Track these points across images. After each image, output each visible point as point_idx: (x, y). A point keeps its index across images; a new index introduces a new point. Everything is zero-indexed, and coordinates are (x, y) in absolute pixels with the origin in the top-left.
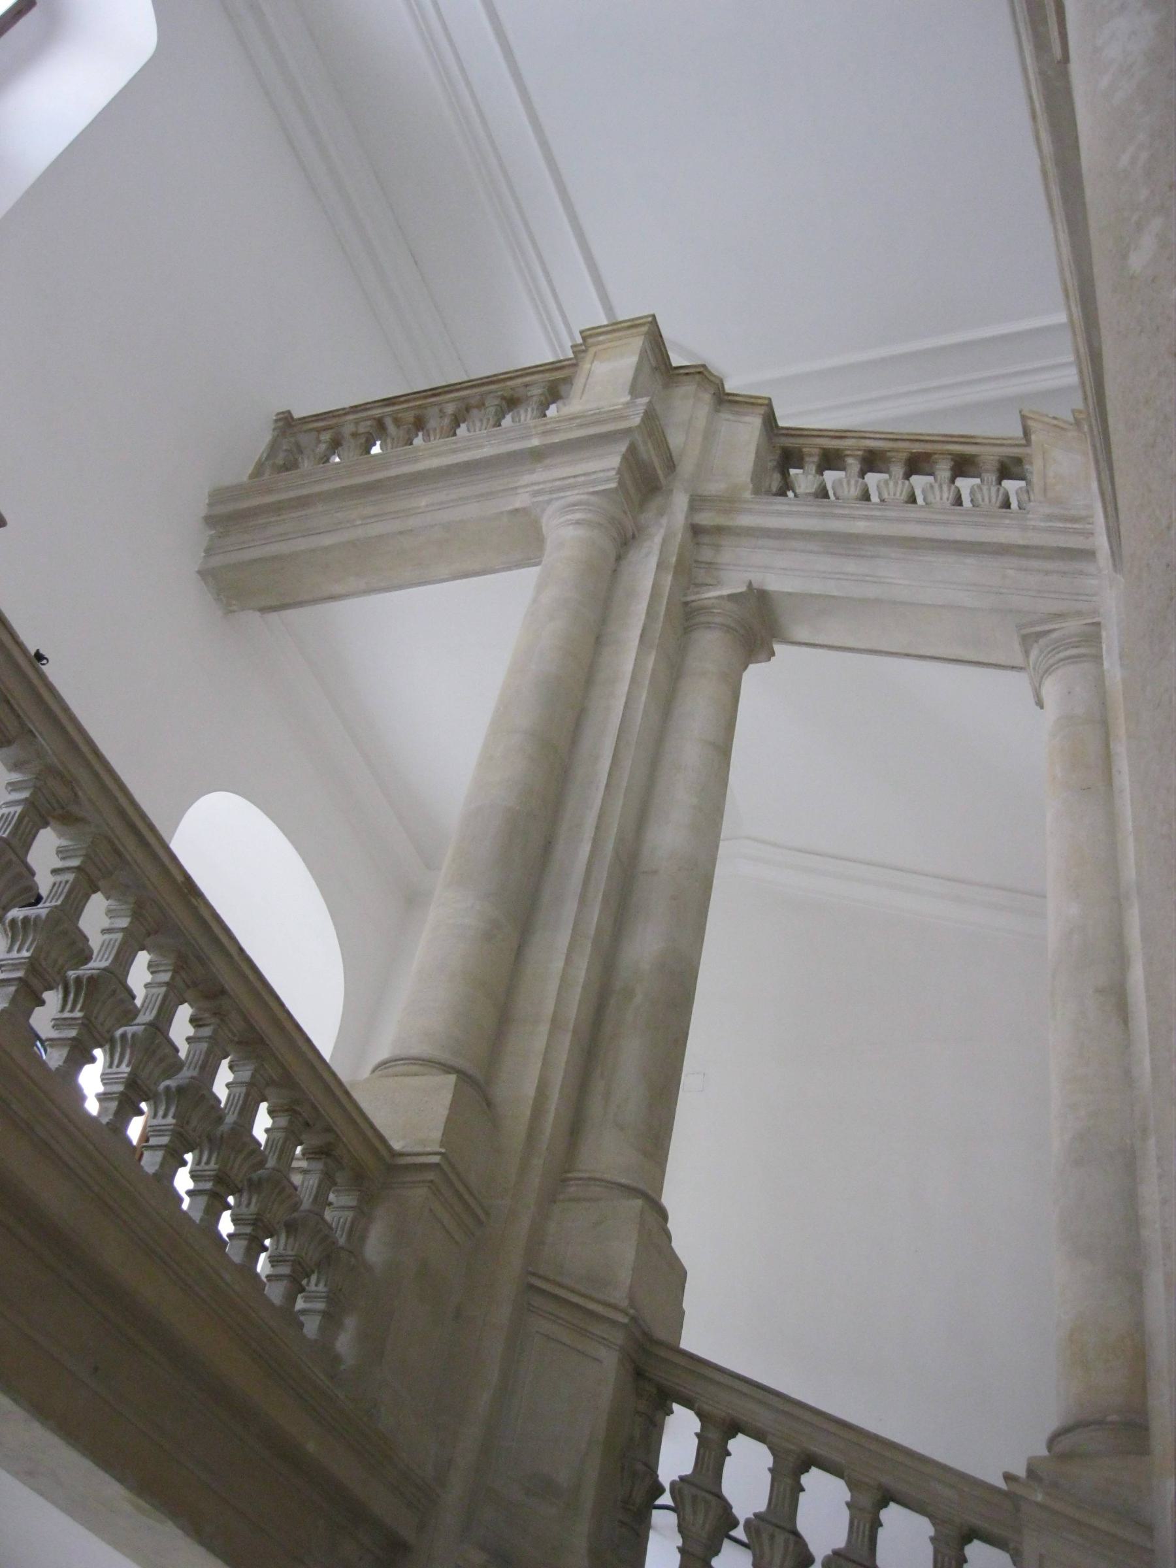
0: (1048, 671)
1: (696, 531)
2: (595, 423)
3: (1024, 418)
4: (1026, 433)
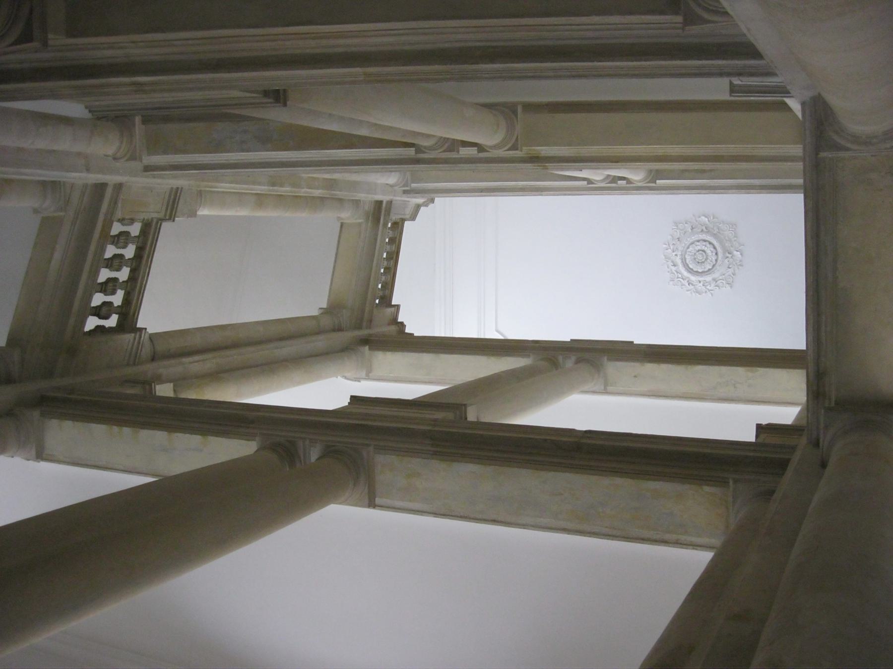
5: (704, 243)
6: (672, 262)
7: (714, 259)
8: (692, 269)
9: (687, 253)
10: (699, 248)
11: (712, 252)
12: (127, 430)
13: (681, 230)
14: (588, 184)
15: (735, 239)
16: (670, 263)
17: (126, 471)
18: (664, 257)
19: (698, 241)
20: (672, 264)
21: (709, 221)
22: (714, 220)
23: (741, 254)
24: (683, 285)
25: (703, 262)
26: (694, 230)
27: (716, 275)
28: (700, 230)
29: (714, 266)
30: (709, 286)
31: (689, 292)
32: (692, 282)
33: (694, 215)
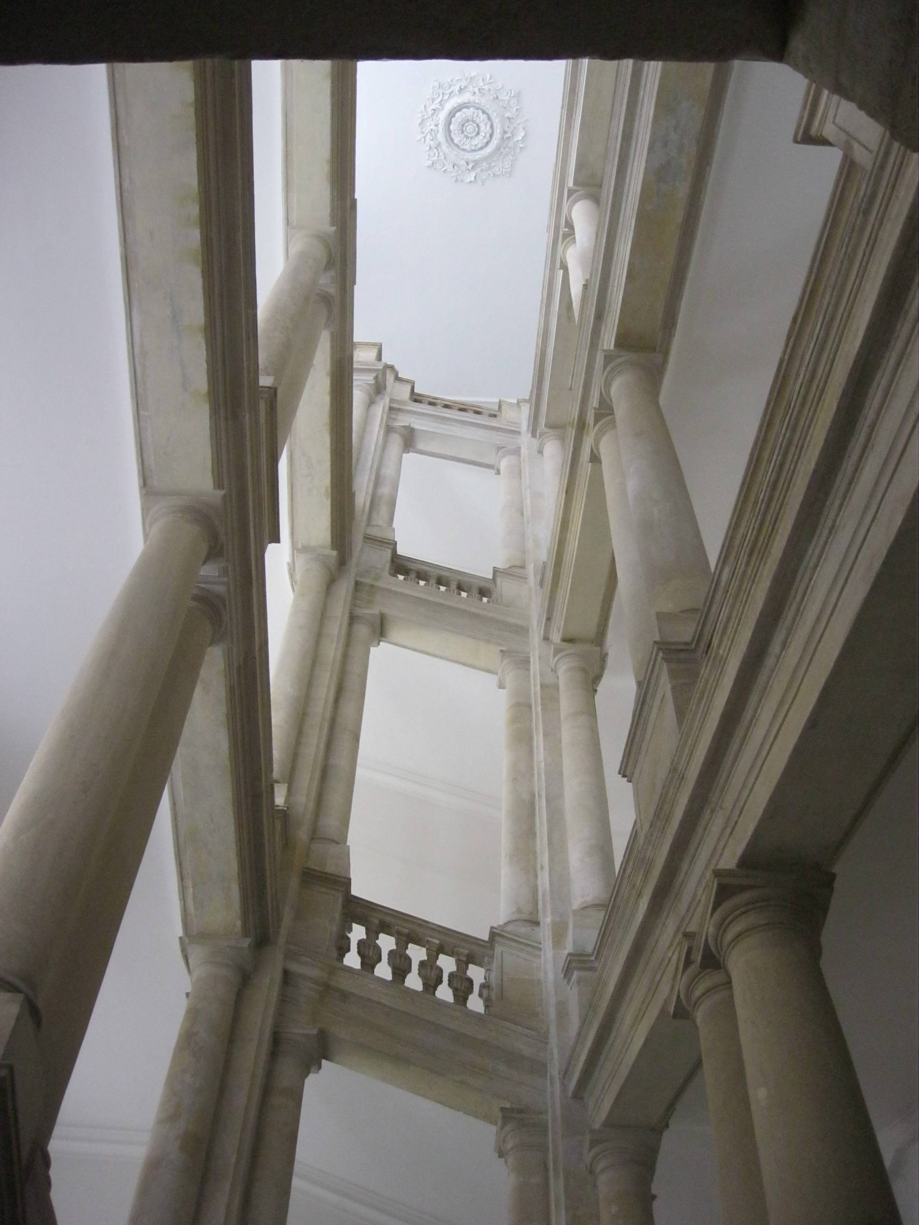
0: (503, 457)
1: (391, 409)
2: (366, 365)
3: (500, 401)
4: (500, 407)
5: (488, 135)
6: (465, 87)
7: (467, 147)
8: (454, 116)
9: (476, 111)
10: (483, 128)
11: (476, 145)
12: (195, 236)
13: (508, 103)
14: (569, 191)
15: (492, 175)
16: (463, 84)
17: (121, 196)
18: (473, 74)
19: (492, 127)
20: (462, 87)
21: (518, 141)
22: (519, 148)
23: (471, 182)
24: (433, 100)
25: (463, 132)
26: (507, 120)
27: (444, 147)
28: (506, 129)
29: (457, 146)
30: (431, 138)
31: (423, 109)
32: (435, 115)
33: (527, 120)
